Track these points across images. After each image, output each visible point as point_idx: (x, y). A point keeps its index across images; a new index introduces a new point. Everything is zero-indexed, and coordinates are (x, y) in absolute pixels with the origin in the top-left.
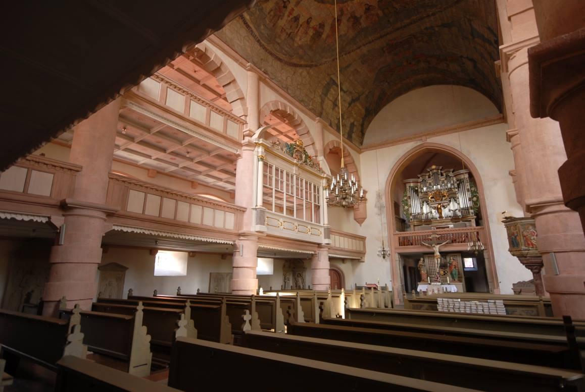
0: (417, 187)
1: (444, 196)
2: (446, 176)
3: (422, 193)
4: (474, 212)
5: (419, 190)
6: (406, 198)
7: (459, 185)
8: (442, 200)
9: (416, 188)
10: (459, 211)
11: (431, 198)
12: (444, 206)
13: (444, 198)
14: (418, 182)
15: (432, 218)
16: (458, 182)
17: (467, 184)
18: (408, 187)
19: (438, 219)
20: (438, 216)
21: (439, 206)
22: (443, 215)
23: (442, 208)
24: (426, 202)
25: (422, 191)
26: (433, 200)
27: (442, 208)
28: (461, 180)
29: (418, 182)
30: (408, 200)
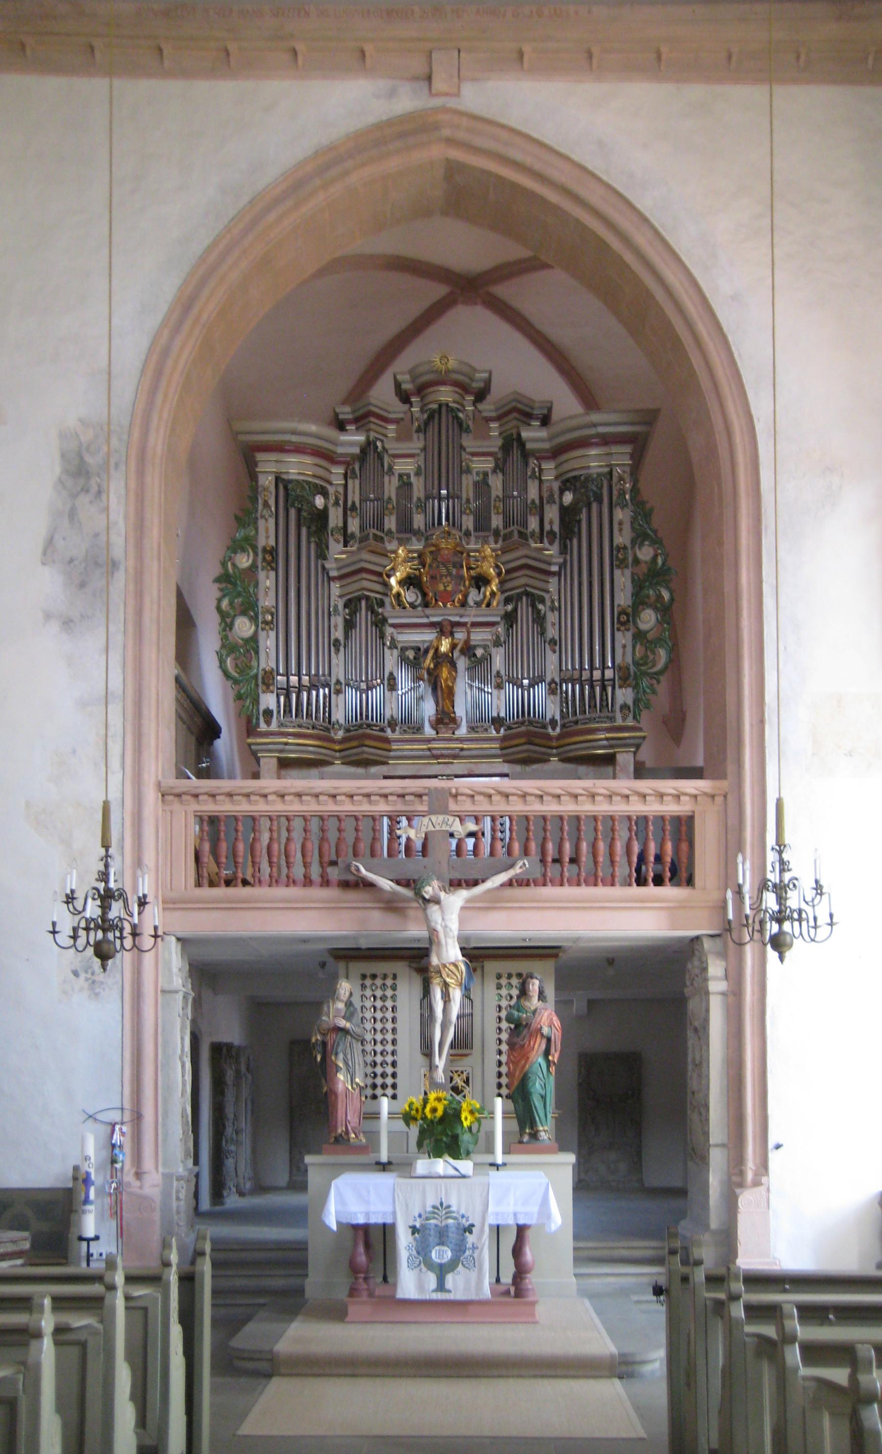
0: (325, 494)
1: (481, 581)
2: (506, 448)
3: (347, 539)
4: (636, 701)
5: (335, 518)
6: (244, 561)
7: (568, 515)
8: (464, 604)
9: (319, 501)
10: (552, 691)
11: (408, 582)
12: (468, 650)
13: (474, 596)
14: (329, 457)
15: (392, 724)
16: (568, 498)
17: (619, 514)
18: (267, 481)
19: (429, 732)
20: (429, 708)
21: (445, 646)
22: (460, 710)
23: (462, 663)
24: (371, 609)
25: (354, 526)
26: (410, 596)
27: (462, 663)
28: (588, 478)
29: (329, 457)
30: (262, 575)
